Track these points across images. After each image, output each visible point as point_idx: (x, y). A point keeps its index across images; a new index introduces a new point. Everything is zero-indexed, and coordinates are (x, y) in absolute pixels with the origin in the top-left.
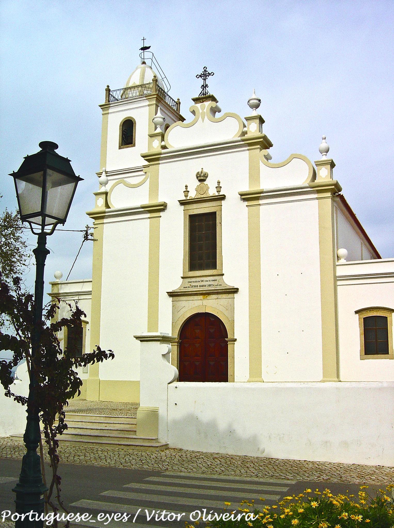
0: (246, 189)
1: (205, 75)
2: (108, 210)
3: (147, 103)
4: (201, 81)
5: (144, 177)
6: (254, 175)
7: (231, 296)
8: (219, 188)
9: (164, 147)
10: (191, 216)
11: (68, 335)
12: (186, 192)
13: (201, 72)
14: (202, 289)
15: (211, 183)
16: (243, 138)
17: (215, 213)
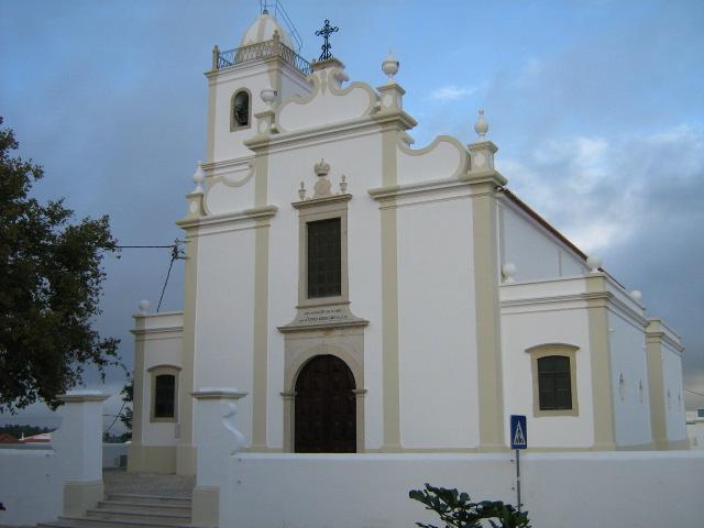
0: (378, 185)
1: (327, 31)
2: (201, 218)
3: (266, 68)
4: (321, 40)
5: (249, 171)
6: (389, 167)
7: (360, 331)
8: (343, 185)
9: (275, 131)
10: (310, 224)
11: (173, 389)
12: (302, 191)
13: (321, 27)
14: (322, 322)
15: (334, 180)
16: (375, 116)
17: (337, 221)
